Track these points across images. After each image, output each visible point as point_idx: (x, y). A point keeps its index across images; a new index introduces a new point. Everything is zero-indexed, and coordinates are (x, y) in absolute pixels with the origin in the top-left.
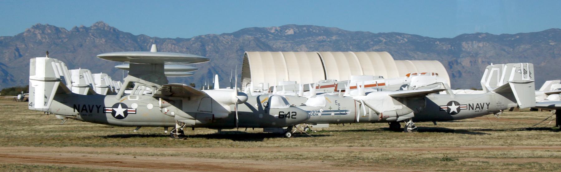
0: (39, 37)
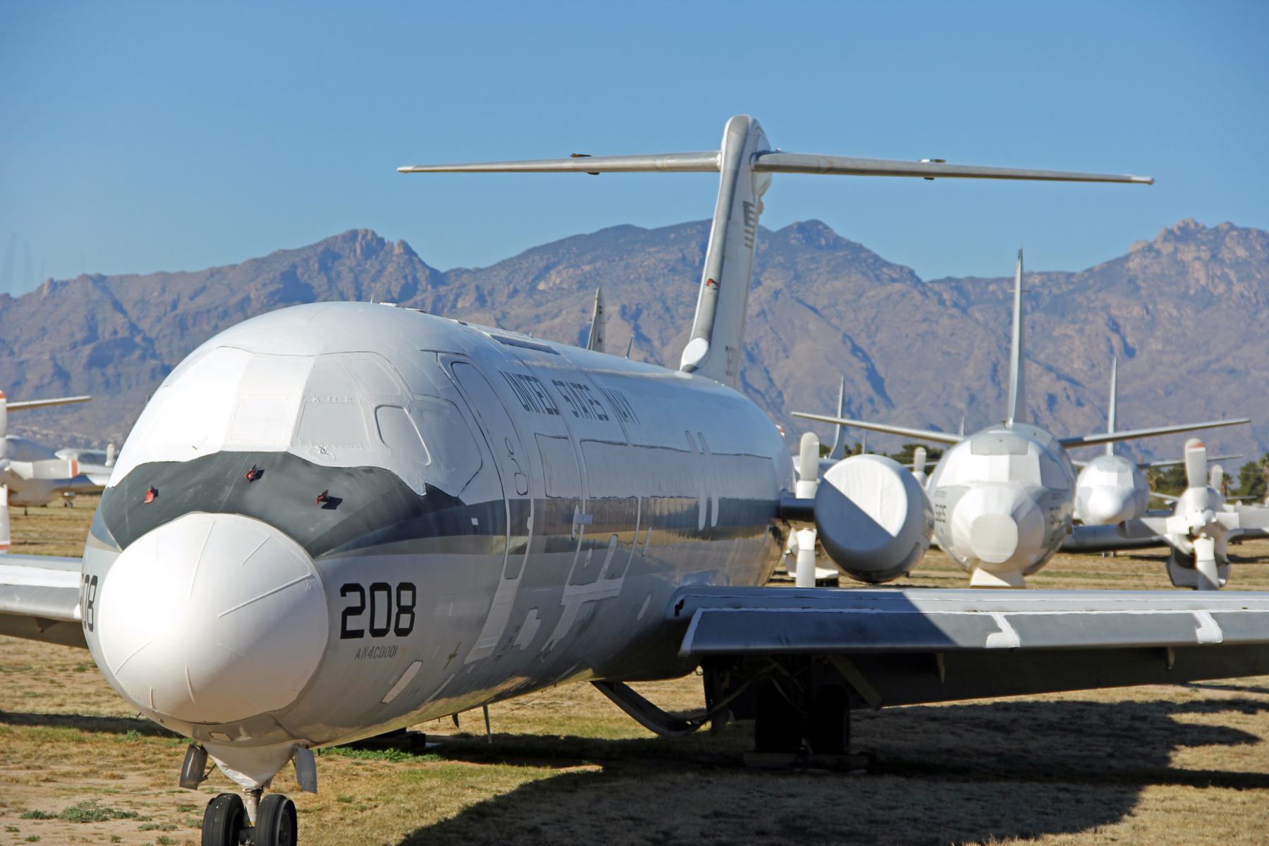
0: (1199, 274)
